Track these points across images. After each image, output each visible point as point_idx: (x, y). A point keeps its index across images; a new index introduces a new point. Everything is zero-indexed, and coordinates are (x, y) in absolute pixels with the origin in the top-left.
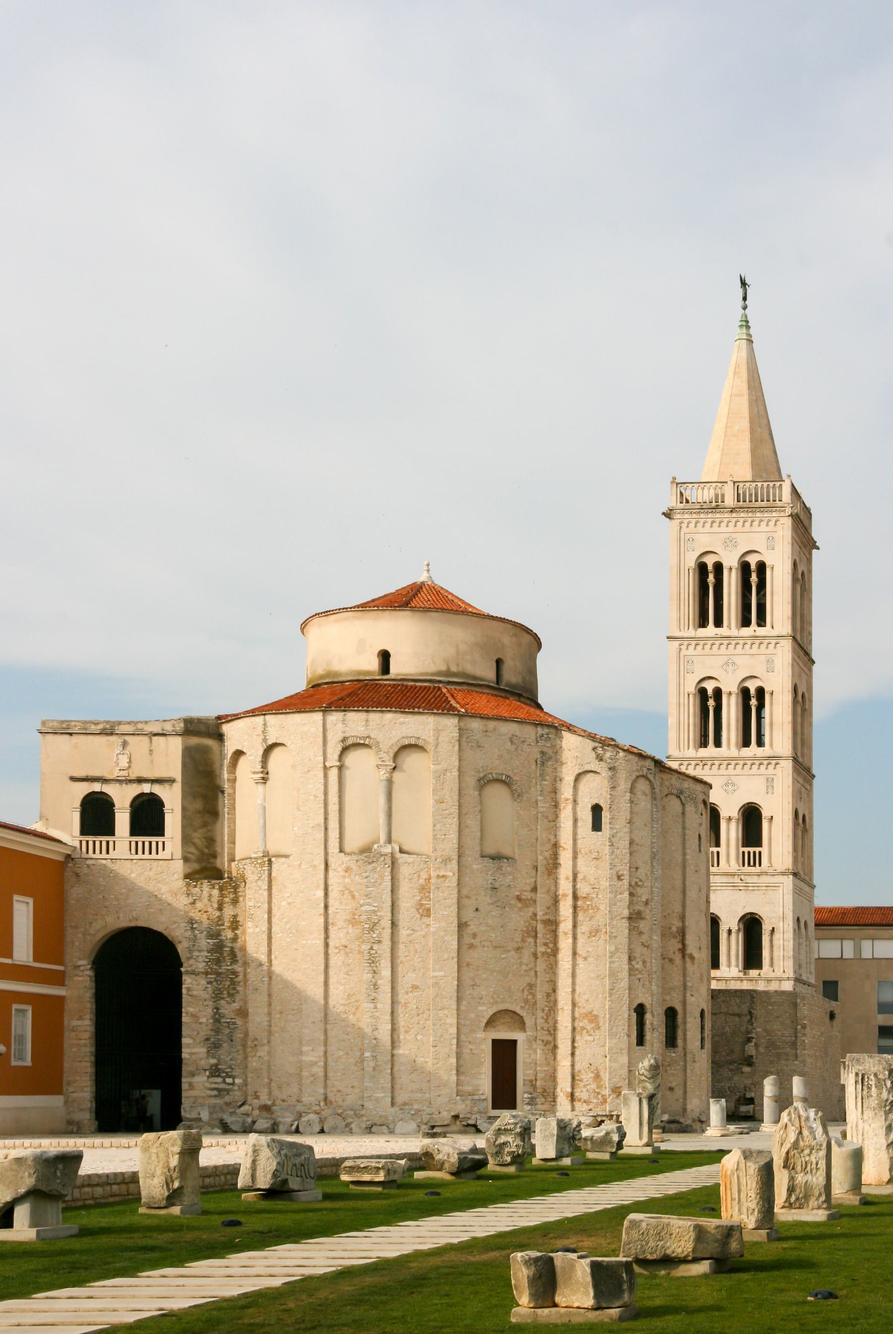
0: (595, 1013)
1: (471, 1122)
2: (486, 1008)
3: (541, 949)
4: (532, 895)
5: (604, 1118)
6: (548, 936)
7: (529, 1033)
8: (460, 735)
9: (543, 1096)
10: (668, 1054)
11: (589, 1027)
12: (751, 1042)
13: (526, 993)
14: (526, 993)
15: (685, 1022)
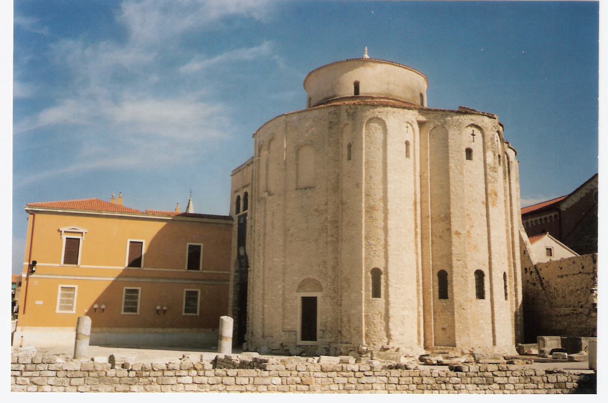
0: (348, 277)
1: (287, 348)
2: (297, 278)
3: (329, 239)
4: (326, 207)
5: (351, 349)
6: (333, 231)
7: (324, 292)
8: (286, 126)
9: (330, 332)
10: (440, 304)
11: (346, 287)
12: (594, 293)
13: (321, 267)
14: (321, 267)
15: (452, 281)
